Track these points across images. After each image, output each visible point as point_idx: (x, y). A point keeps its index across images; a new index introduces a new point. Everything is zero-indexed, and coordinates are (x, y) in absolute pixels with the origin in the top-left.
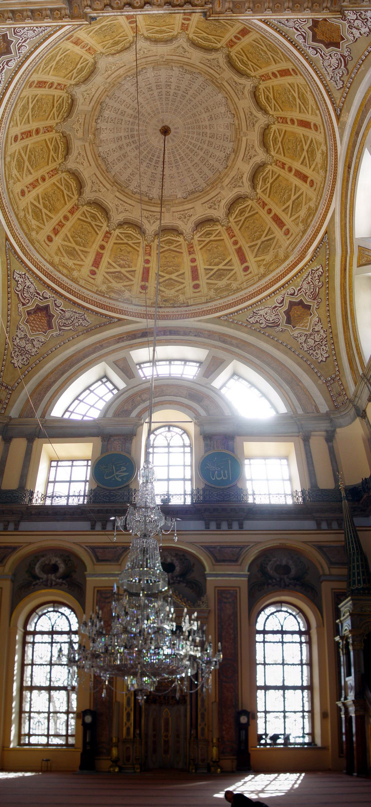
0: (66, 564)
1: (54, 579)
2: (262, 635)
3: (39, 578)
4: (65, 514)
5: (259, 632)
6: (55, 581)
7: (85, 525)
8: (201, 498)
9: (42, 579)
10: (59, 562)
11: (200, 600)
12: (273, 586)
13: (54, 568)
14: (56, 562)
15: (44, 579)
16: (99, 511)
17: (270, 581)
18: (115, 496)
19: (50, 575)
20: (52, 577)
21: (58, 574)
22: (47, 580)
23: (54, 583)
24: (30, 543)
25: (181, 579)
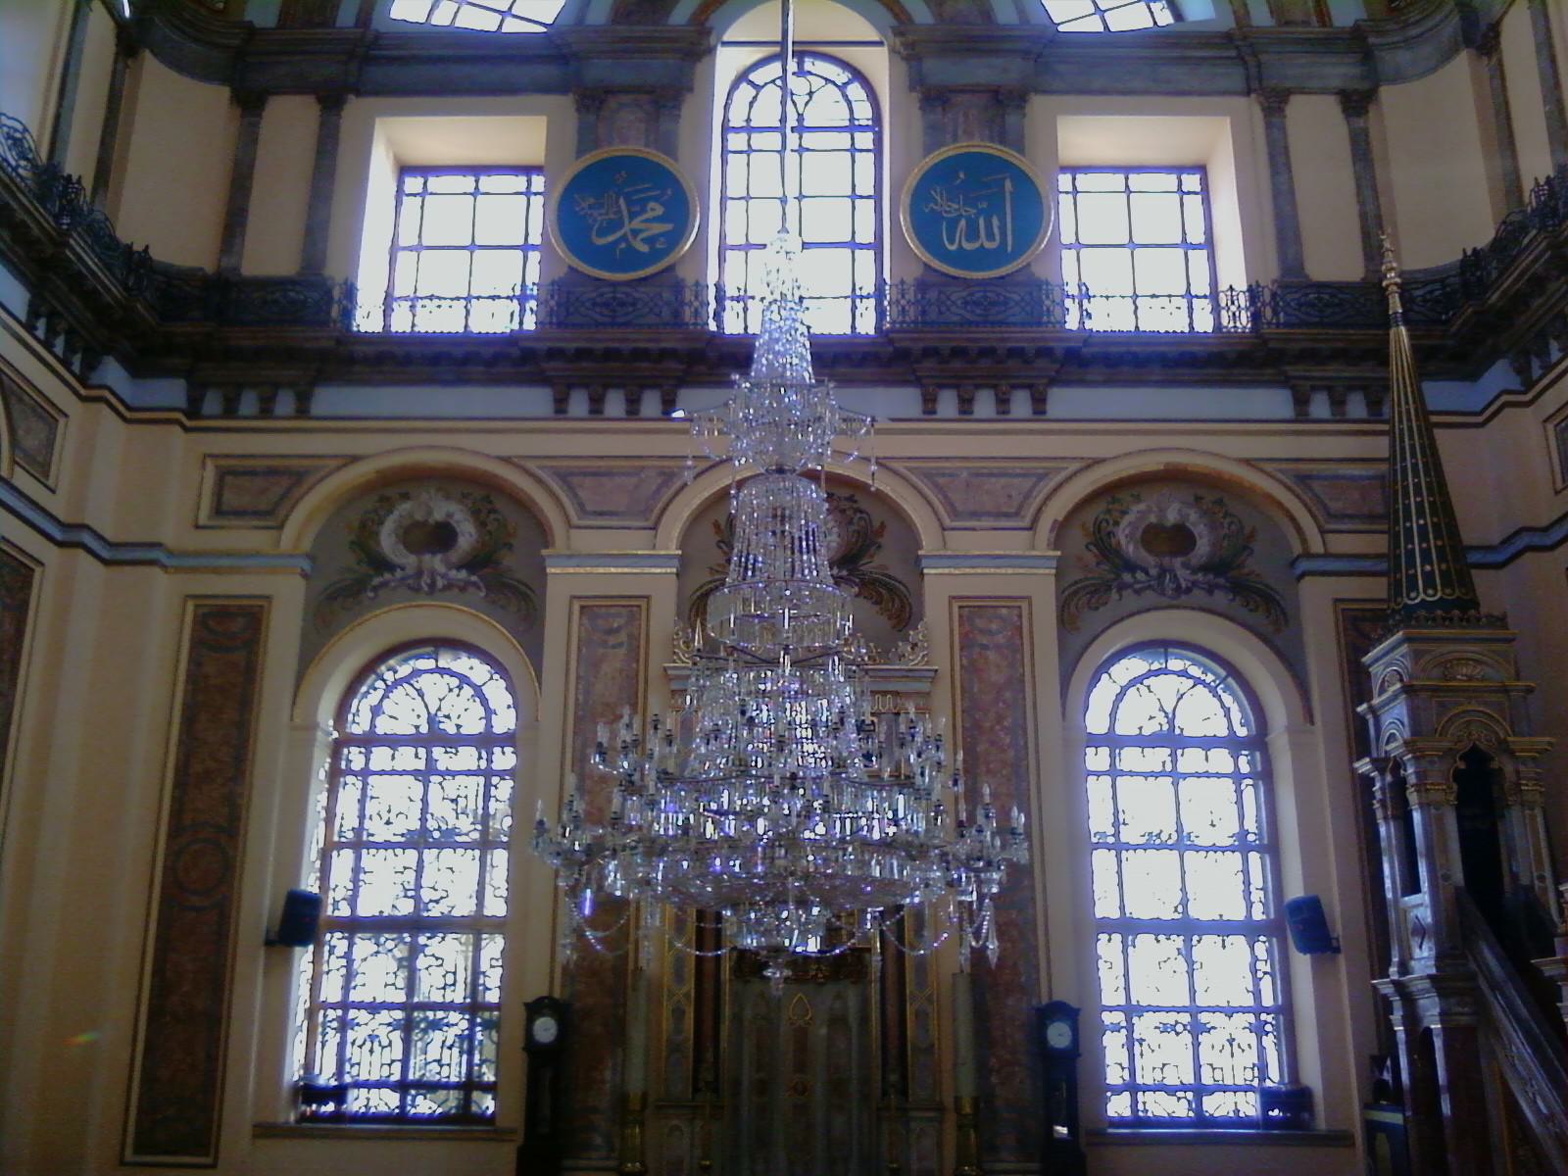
0: (482, 525)
1: (440, 568)
2: (1104, 751)
3: (390, 567)
4: (467, 359)
5: (1095, 741)
6: (443, 576)
7: (536, 400)
8: (912, 312)
9: (403, 569)
10: (458, 516)
11: (906, 639)
12: (1138, 592)
13: (442, 537)
14: (450, 515)
15: (410, 571)
16: (581, 354)
17: (1127, 577)
18: (634, 304)
19: (427, 557)
20: (436, 562)
21: (455, 555)
22: (419, 573)
23: (440, 583)
24: (355, 459)
25: (844, 573)
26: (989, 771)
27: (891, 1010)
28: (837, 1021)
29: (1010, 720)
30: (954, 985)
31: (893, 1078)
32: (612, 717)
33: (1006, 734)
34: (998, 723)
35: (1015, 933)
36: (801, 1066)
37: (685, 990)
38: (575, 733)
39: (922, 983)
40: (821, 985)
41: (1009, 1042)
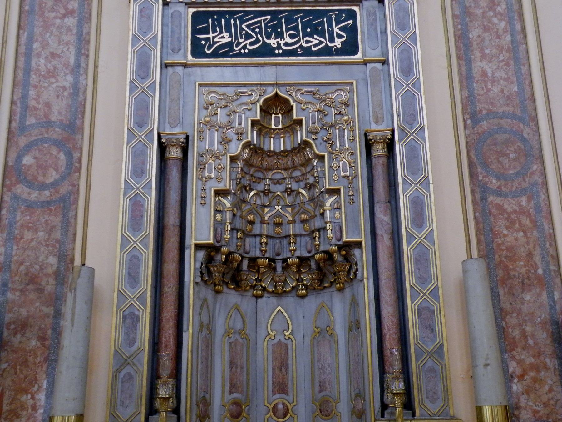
26: (483, 57)
27: (388, 311)
28: (323, 333)
29: (504, 6)
30: (465, 271)
31: (399, 386)
32: (62, 11)
33: (500, 20)
34: (490, 9)
35: (526, 221)
36: (281, 387)
37: (139, 291)
38: (19, 27)
39: (423, 278)
40: (303, 297)
41: (531, 342)
